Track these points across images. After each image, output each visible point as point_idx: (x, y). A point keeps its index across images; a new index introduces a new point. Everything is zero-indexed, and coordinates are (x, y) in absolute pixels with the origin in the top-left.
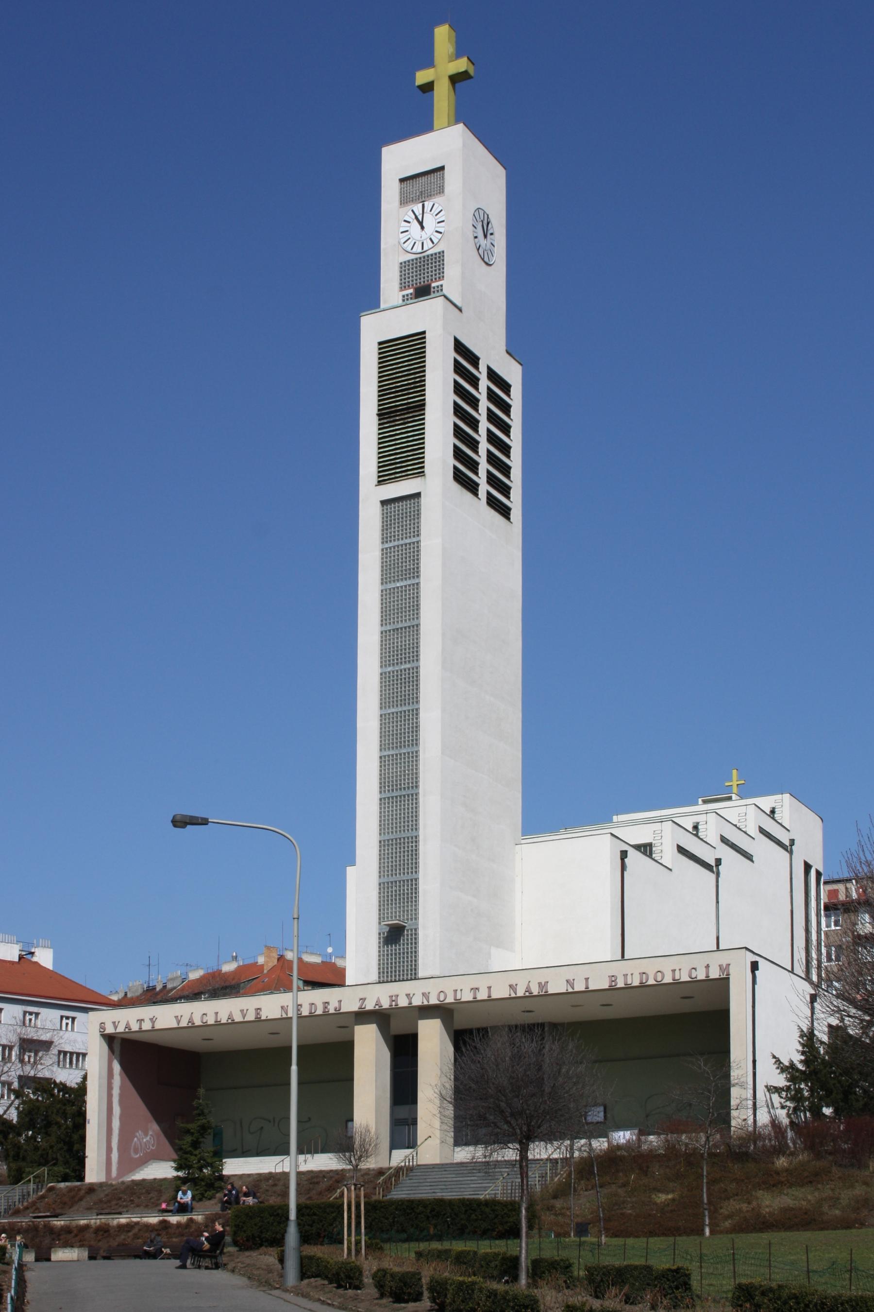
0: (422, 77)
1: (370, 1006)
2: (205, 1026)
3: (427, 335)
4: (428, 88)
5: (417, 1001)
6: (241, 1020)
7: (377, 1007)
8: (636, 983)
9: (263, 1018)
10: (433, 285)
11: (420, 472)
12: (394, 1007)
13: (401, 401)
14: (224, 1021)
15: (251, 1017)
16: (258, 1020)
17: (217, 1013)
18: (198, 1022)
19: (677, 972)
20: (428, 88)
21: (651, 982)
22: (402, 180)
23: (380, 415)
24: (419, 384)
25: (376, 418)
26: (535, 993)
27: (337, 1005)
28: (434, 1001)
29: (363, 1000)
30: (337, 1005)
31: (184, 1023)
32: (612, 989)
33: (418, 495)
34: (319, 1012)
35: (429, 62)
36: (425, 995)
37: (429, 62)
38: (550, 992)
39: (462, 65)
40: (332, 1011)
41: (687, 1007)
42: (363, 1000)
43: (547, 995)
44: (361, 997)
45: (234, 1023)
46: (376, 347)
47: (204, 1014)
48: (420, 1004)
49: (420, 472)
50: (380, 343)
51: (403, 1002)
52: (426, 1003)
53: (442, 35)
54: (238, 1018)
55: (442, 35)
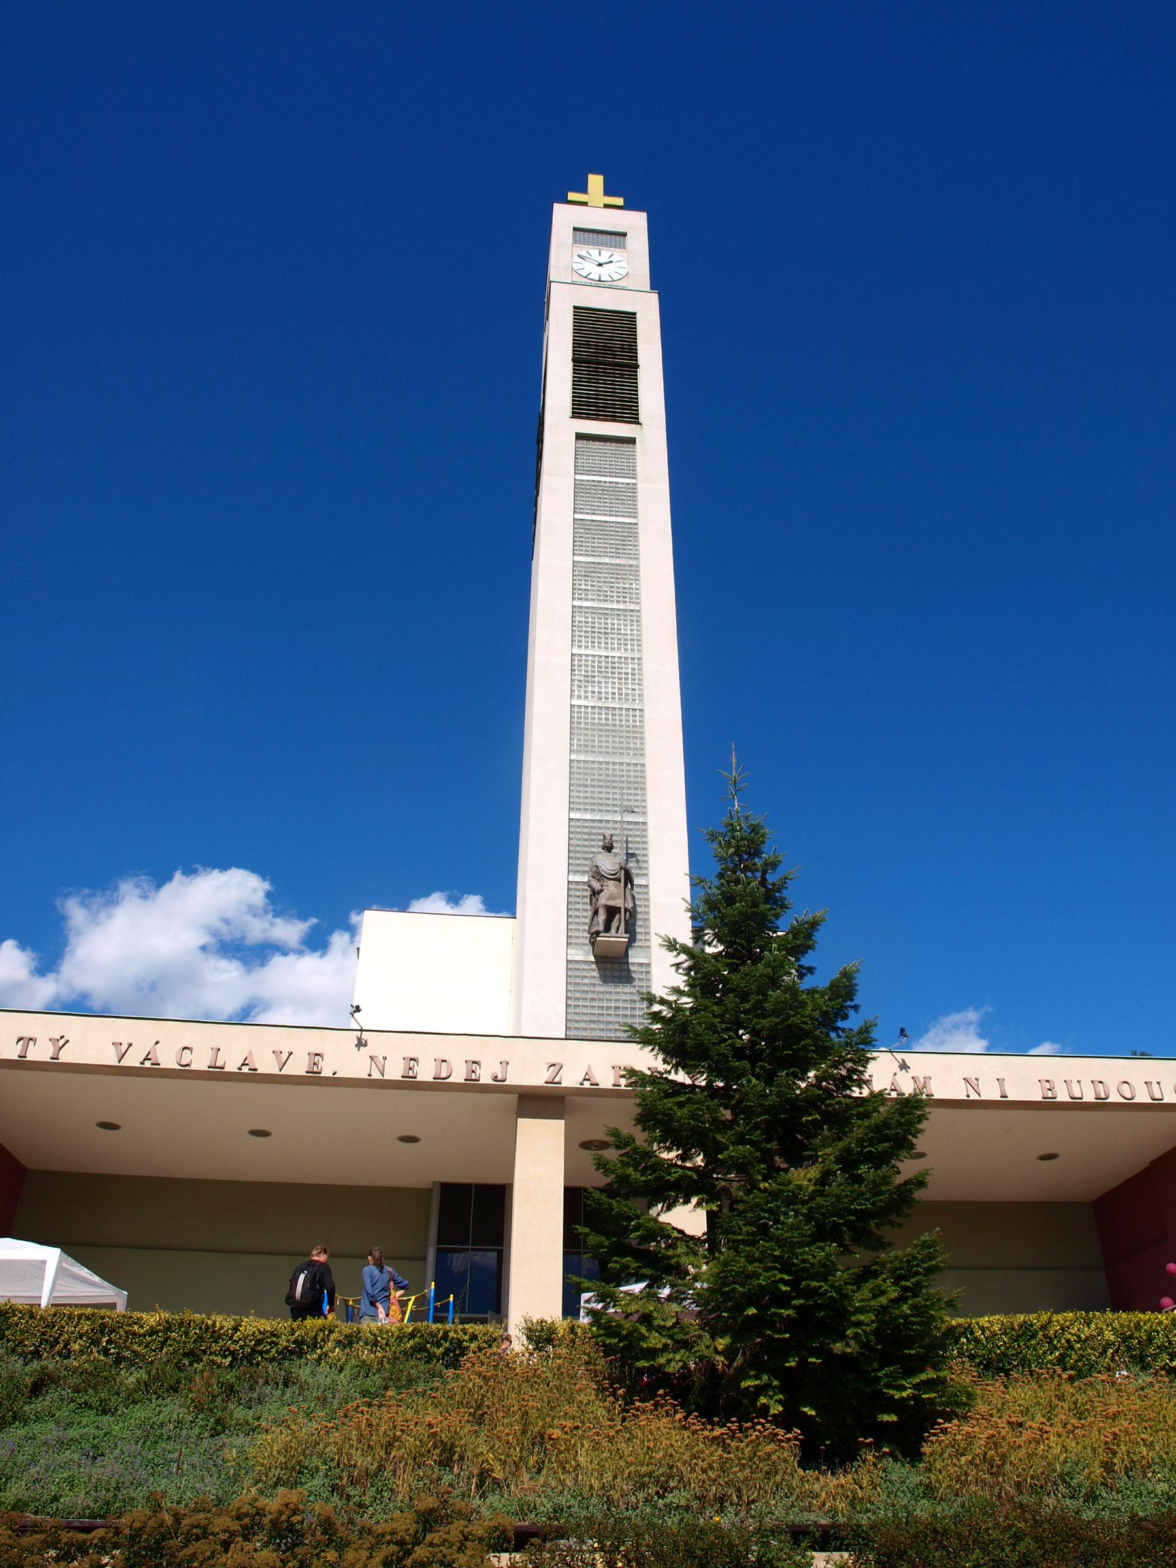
1: (570, 1079)
6: (275, 1070)
7: (587, 1085)
11: (634, 419)
12: (623, 1087)
14: (231, 1067)
19: (1155, 1087)
22: (575, 229)
23: (574, 360)
25: (571, 364)
33: (632, 441)
38: (938, 1095)
44: (553, 1062)
46: (571, 310)
47: (185, 1048)
49: (634, 419)
50: (575, 308)
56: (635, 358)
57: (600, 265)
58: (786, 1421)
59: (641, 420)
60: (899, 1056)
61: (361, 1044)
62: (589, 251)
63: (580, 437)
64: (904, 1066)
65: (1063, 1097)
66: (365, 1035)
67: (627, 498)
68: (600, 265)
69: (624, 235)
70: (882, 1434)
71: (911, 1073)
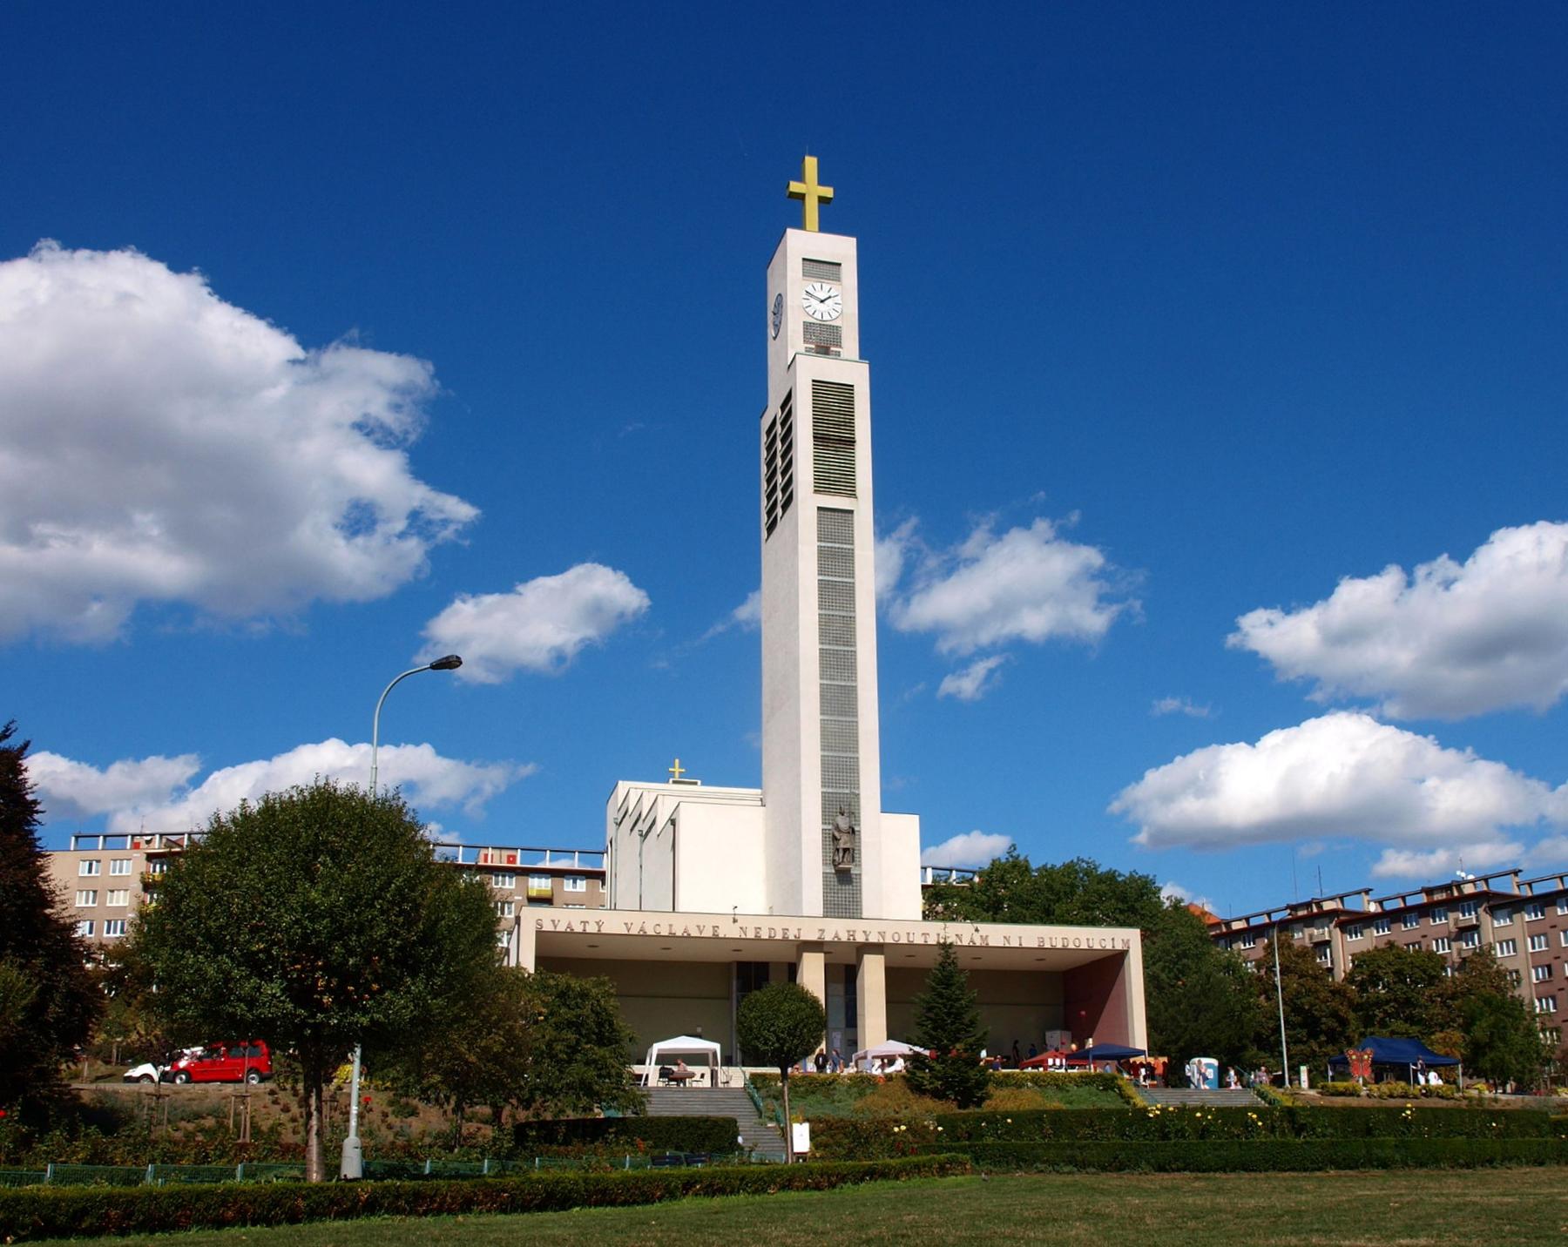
0: (795, 187)
1: (828, 937)
2: (658, 936)
3: (855, 388)
4: (802, 197)
5: (873, 939)
8: (1060, 946)
9: (721, 935)
10: (832, 349)
13: (833, 432)
15: (708, 933)
16: (716, 937)
17: (671, 926)
18: (650, 932)
20: (802, 197)
21: (1071, 946)
22: (804, 259)
24: (850, 424)
26: (978, 944)
27: (796, 933)
28: (889, 940)
29: (822, 931)
30: (796, 933)
31: (634, 931)
32: (1041, 949)
33: (851, 512)
34: (779, 936)
35: (800, 178)
36: (882, 934)
37: (800, 178)
38: (991, 944)
39: (828, 192)
40: (792, 937)
41: (1042, 966)
42: (822, 931)
43: (987, 947)
45: (689, 936)
48: (876, 941)
50: (814, 381)
51: (860, 938)
52: (881, 941)
53: (811, 163)
54: (694, 933)
55: (811, 163)
56: (852, 431)
57: (822, 301)
58: (955, 1099)
59: (858, 495)
60: (975, 925)
61: (735, 921)
62: (815, 285)
63: (819, 509)
64: (977, 930)
65: (1047, 945)
66: (736, 917)
67: (848, 557)
68: (822, 301)
69: (839, 265)
70: (974, 1102)
71: (981, 933)
